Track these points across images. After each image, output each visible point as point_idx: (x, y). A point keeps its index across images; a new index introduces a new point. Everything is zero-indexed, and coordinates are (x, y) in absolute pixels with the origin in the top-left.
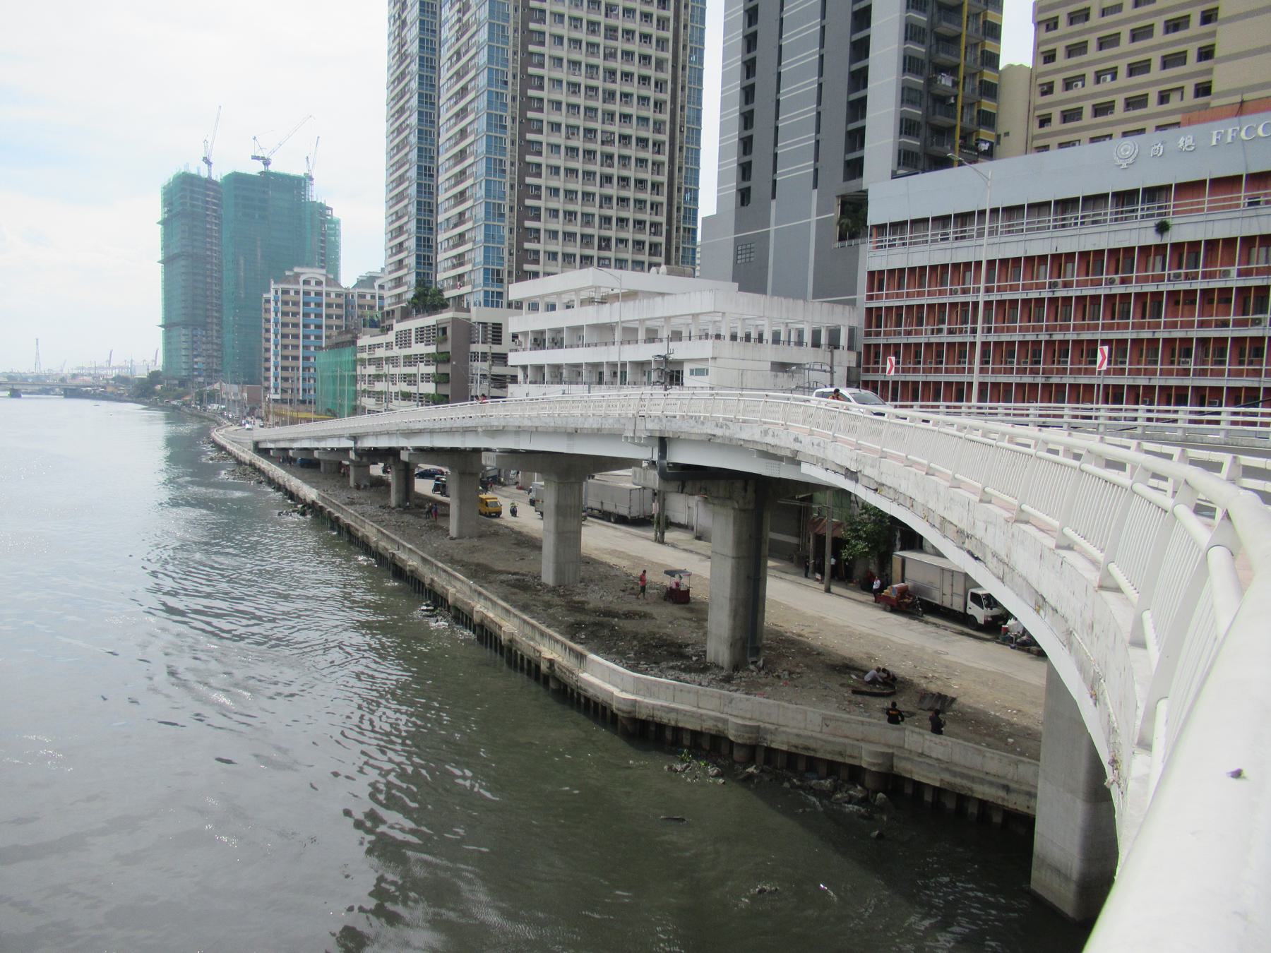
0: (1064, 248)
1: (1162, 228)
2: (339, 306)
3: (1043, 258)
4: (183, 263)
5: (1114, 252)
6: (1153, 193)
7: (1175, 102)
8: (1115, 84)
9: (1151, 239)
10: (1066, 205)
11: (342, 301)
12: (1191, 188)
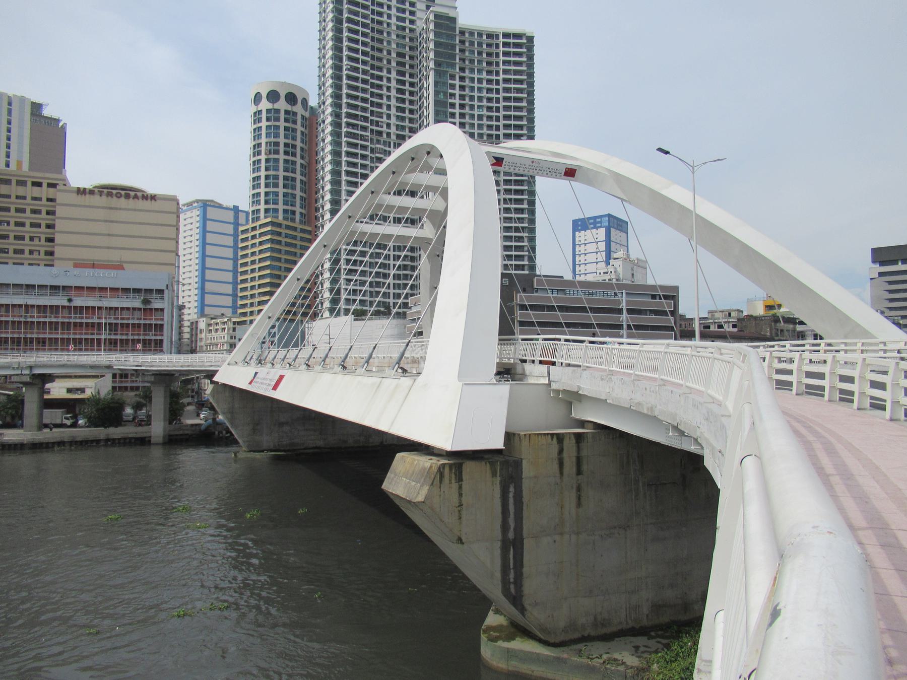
0: (30, 302)
1: (70, 300)
3: (20, 306)
5: (51, 307)
6: (64, 287)
7: (36, 242)
8: (8, 228)
9: (66, 303)
10: (29, 287)
12: (79, 289)
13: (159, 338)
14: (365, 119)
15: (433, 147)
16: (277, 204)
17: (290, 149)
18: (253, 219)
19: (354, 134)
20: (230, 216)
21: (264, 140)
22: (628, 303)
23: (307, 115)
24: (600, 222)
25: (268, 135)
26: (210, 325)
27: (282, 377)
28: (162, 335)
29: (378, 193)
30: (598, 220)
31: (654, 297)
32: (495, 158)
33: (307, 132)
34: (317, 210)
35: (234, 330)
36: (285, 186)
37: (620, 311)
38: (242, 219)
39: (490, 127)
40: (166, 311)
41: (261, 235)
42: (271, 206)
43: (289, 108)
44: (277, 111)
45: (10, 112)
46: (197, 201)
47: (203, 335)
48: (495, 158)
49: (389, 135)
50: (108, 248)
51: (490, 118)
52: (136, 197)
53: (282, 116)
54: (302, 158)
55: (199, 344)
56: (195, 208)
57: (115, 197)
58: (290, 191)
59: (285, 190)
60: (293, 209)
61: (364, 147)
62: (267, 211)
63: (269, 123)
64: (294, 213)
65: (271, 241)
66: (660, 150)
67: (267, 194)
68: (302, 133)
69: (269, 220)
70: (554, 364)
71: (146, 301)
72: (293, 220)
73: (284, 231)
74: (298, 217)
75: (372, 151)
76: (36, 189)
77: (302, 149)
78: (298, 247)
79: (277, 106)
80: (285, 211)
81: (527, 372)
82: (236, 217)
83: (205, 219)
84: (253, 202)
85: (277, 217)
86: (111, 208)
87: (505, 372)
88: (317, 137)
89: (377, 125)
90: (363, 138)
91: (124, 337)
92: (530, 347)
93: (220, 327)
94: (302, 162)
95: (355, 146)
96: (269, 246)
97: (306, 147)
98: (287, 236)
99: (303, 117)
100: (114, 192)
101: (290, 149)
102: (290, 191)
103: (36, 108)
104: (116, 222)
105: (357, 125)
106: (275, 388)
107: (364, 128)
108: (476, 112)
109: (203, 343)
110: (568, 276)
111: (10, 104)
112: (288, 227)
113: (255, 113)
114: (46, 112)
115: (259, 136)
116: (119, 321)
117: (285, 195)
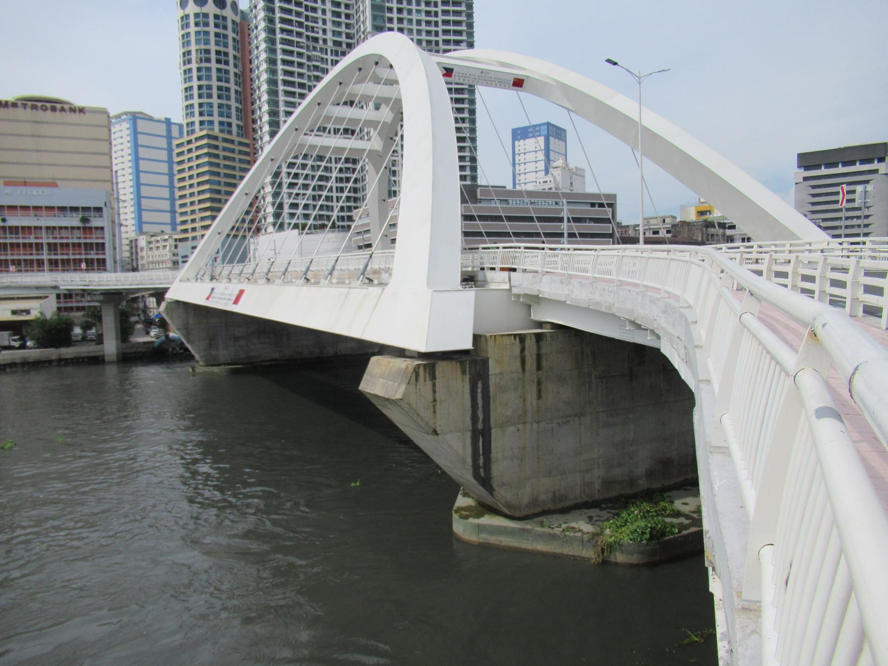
13: (101, 257)
14: (300, 24)
15: (381, 57)
16: (211, 115)
17: (222, 58)
18: (188, 132)
19: (290, 40)
20: (162, 129)
21: (193, 47)
22: (570, 211)
23: (238, 19)
24: (539, 131)
25: (198, 42)
26: (150, 243)
27: (242, 292)
28: (104, 254)
29: (326, 105)
30: (537, 129)
31: (593, 205)
32: (445, 68)
33: (238, 38)
34: (254, 121)
35: (176, 247)
36: (219, 97)
37: (561, 220)
38: (175, 132)
39: (429, 33)
40: (106, 229)
41: (197, 148)
42: (206, 118)
43: (218, 12)
44: (206, 15)
46: (126, 113)
47: (144, 254)
48: (445, 68)
49: (325, 41)
50: (38, 164)
51: (428, 23)
52: (63, 110)
53: (211, 20)
54: (235, 66)
55: (140, 263)
56: (124, 120)
57: (40, 111)
58: (224, 102)
59: (220, 101)
60: (229, 120)
61: (300, 55)
62: (202, 123)
63: (198, 29)
64: (230, 125)
65: (208, 154)
66: (609, 61)
67: (201, 105)
68: (234, 39)
69: (204, 133)
70: (514, 270)
71: (85, 220)
72: (230, 132)
73: (221, 144)
74: (234, 129)
75: (309, 58)
77: (235, 57)
78: (237, 160)
79: (205, 10)
80: (221, 123)
81: (489, 279)
82: (169, 131)
83: (135, 133)
84: (187, 114)
85: (213, 129)
86: (36, 122)
87: (469, 279)
88: (250, 44)
89: (313, 31)
90: (298, 45)
91: (65, 257)
92: (495, 253)
93: (160, 244)
94: (236, 70)
95: (291, 53)
96: (206, 159)
97: (239, 55)
98: (224, 149)
99: (234, 22)
100: (39, 104)
101: (222, 58)
102: (224, 102)
104: (44, 137)
105: (292, 31)
106: (236, 301)
107: (299, 35)
108: (414, 17)
109: (144, 262)
110: (510, 187)
112: (225, 140)
113: (182, 18)
115: (188, 43)
116: (58, 241)
117: (220, 106)
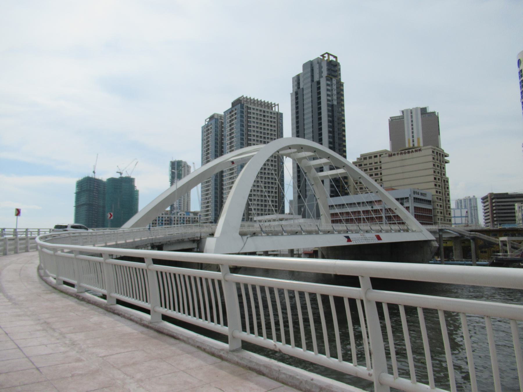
1: (372, 207)
2: (168, 221)
4: (85, 207)
11: (169, 219)
40: (410, 208)
45: (412, 116)
52: (412, 152)
76: (376, 158)
86: (403, 160)
100: (403, 152)
103: (424, 111)
111: (411, 113)
114: (430, 110)
